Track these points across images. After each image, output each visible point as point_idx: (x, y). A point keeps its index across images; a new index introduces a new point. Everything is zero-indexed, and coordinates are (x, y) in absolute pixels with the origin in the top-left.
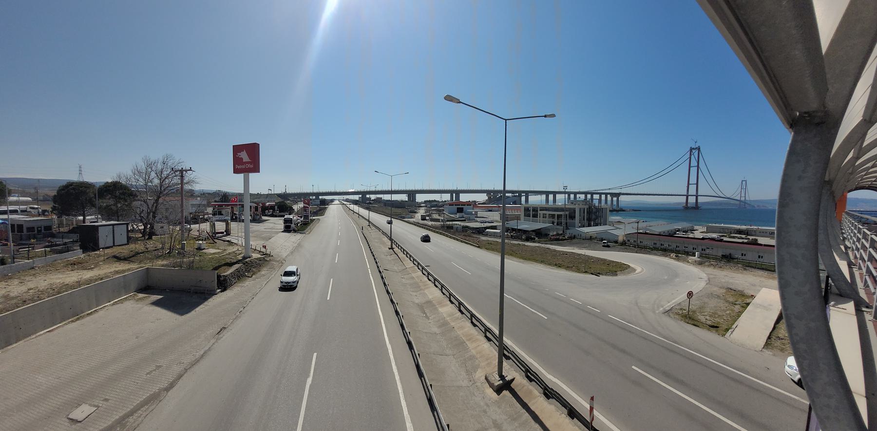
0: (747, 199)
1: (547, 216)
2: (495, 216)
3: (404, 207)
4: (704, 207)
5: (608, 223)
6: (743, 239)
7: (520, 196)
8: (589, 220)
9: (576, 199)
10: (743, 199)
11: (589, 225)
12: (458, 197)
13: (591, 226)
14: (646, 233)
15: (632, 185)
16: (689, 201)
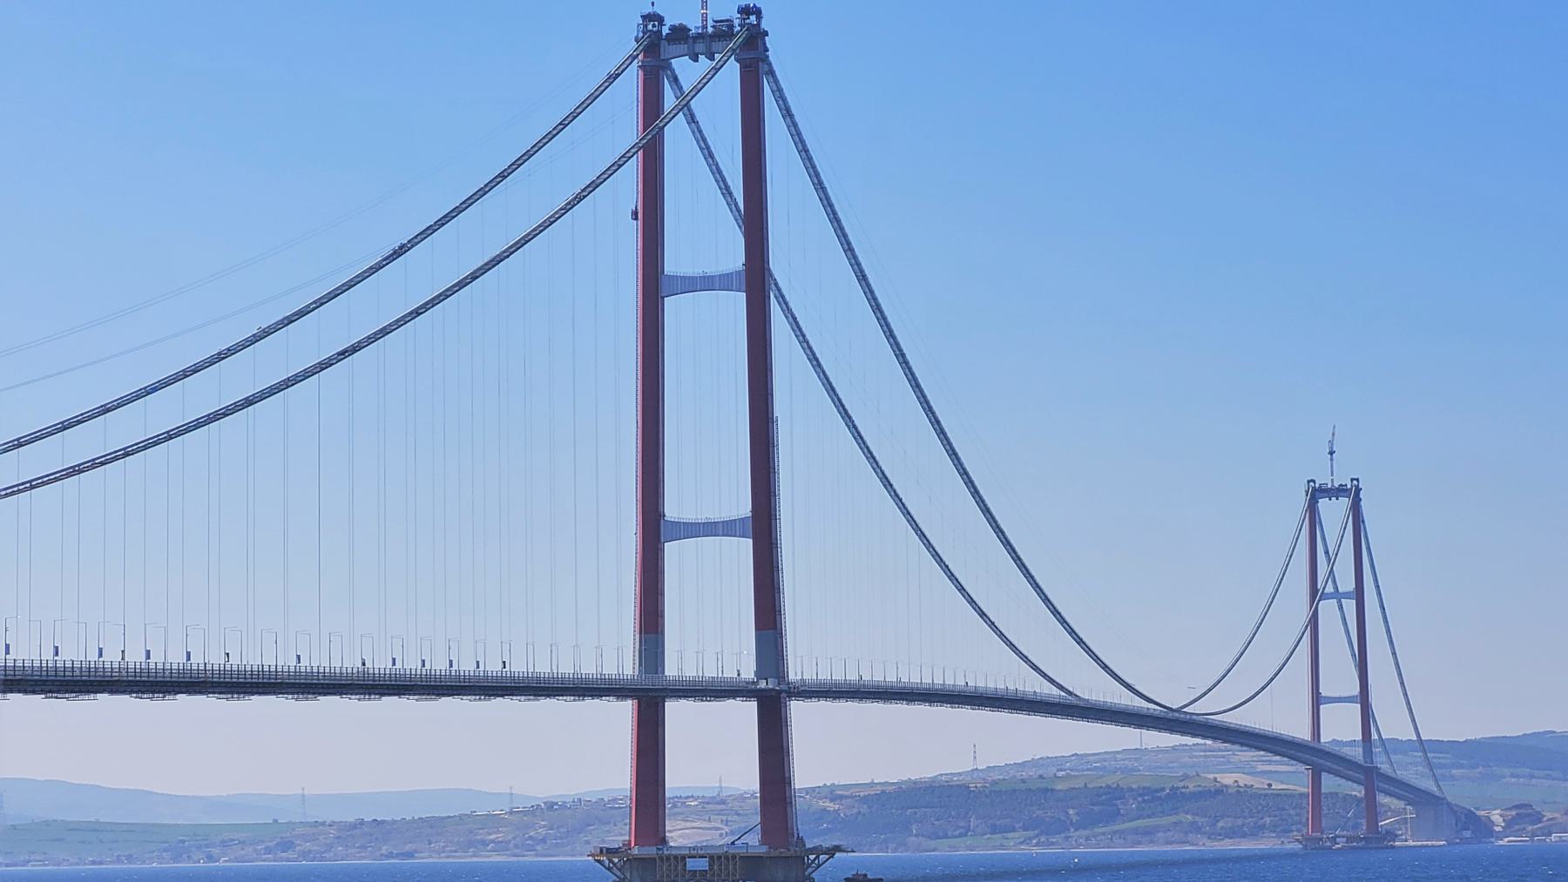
0: (1392, 725)
10: (1341, 727)
16: (679, 776)
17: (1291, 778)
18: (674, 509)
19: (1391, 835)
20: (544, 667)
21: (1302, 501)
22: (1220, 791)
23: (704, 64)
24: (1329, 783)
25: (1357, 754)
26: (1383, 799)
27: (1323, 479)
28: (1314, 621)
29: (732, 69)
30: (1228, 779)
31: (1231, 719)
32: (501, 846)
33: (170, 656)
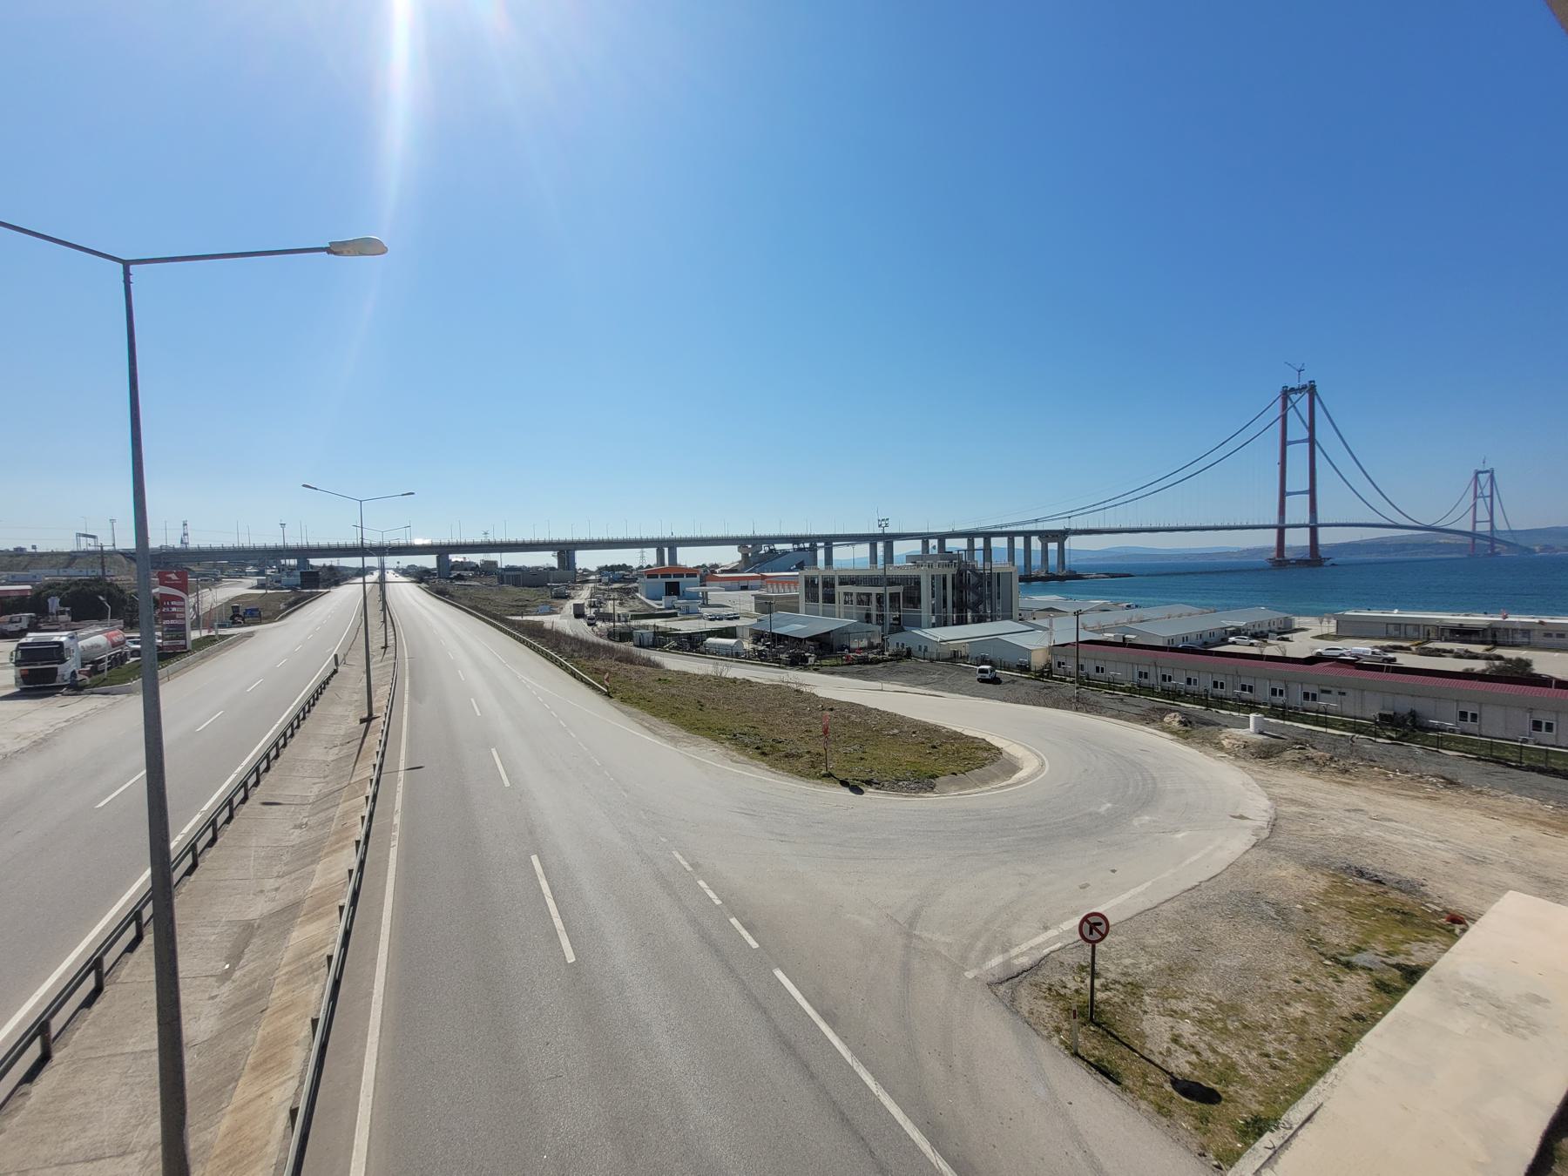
0: (1500, 525)
1: (854, 597)
2: (743, 603)
3: (542, 585)
4: (1336, 560)
5: (1015, 615)
6: (1475, 657)
7: (814, 549)
8: (960, 606)
9: (928, 552)
10: (1483, 528)
11: (961, 621)
12: (673, 556)
13: (966, 623)
14: (1124, 644)
15: (1094, 508)
16: (1287, 543)
17: (1467, 540)
18: (1288, 489)
19: (1499, 553)
20: (1256, 523)
21: (1473, 475)
22: (1439, 544)
23: (1299, 395)
24: (1477, 541)
25: (1488, 534)
26: (1496, 545)
27: (1481, 469)
28: (1475, 505)
29: (1307, 395)
30: (1441, 541)
31: (1449, 527)
32: (1236, 558)
33: (1173, 525)
